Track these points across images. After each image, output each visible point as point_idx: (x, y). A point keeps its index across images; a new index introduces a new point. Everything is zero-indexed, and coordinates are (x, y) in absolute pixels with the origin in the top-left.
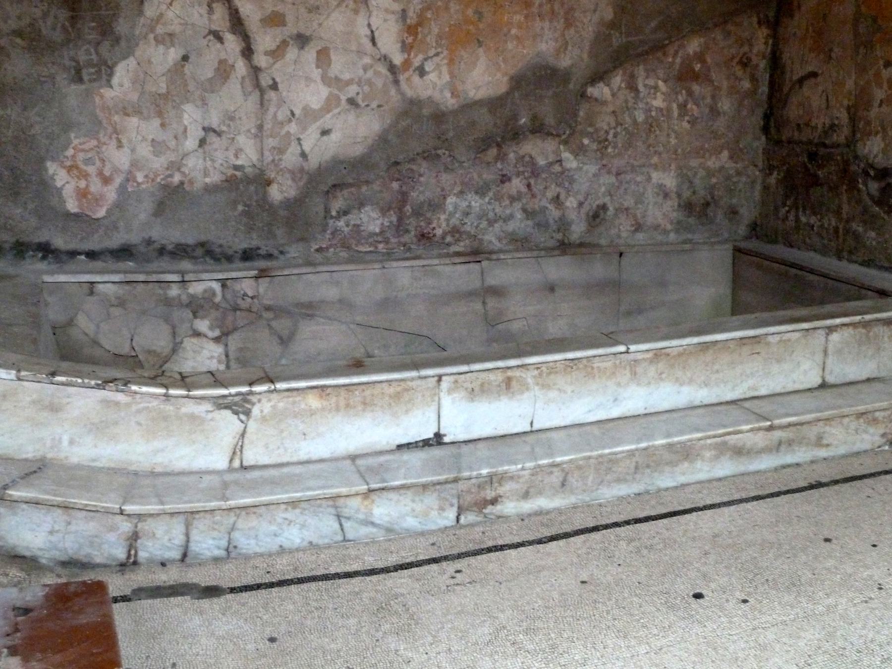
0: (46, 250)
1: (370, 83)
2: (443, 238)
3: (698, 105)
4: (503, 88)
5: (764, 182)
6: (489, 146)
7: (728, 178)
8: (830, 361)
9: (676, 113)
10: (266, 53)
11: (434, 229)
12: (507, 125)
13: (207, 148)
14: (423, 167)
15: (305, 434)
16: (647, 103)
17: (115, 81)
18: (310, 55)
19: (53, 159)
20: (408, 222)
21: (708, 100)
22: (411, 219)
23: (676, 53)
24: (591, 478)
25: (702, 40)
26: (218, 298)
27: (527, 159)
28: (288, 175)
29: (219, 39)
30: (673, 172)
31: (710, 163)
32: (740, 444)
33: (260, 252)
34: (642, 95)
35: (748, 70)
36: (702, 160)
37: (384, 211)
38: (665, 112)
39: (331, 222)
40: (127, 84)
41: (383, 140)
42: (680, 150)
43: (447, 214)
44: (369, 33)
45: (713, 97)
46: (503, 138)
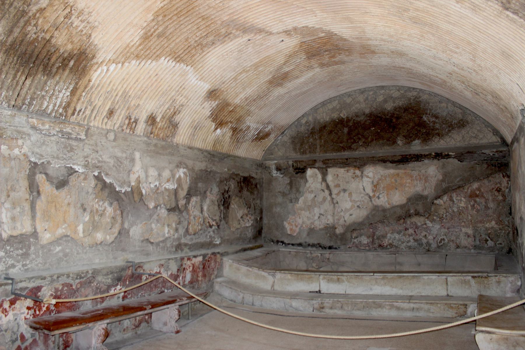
0: (283, 242)
1: (363, 201)
2: (387, 246)
3: (479, 206)
6: (401, 219)
7: (496, 231)
8: (449, 287)
9: (470, 208)
10: (335, 194)
12: (406, 212)
14: (380, 225)
16: (458, 205)
17: (299, 202)
18: (347, 194)
21: (484, 203)
23: (468, 188)
24: (350, 307)
25: (479, 184)
27: (414, 223)
28: (341, 226)
29: (323, 191)
31: (487, 225)
32: (398, 306)
34: (455, 203)
35: (501, 193)
36: (483, 224)
37: (368, 237)
39: (353, 240)
40: (302, 203)
41: (367, 217)
45: (486, 202)
46: (405, 217)
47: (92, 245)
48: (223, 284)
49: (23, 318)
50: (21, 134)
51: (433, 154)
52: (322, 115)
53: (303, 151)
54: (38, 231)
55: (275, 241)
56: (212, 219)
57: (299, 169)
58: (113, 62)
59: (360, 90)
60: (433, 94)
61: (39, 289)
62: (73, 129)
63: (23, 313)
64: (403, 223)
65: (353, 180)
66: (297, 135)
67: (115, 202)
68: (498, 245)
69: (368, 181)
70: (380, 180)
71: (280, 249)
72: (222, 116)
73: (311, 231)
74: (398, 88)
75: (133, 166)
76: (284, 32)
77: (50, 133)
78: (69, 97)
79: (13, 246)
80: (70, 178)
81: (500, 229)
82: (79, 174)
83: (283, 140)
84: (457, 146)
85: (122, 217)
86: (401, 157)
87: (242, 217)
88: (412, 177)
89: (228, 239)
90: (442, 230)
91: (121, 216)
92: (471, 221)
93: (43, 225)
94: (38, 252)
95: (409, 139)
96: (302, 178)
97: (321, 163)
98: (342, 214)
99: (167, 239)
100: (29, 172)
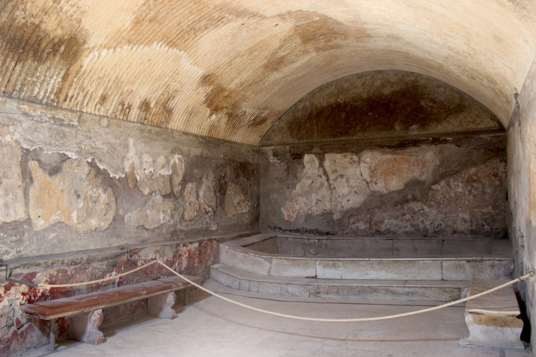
0: (280, 229)
1: (360, 187)
3: (476, 191)
4: (402, 187)
6: (398, 205)
7: (492, 216)
8: (444, 272)
10: (333, 180)
12: (404, 198)
13: (317, 205)
14: (377, 210)
16: (455, 190)
17: (296, 188)
18: (344, 180)
19: (283, 207)
21: (481, 189)
23: (465, 173)
25: (476, 169)
26: (317, 244)
29: (321, 177)
30: (467, 214)
31: (483, 211)
34: (452, 188)
35: (497, 178)
37: (366, 223)
38: (463, 193)
39: (350, 226)
40: (299, 189)
41: (365, 203)
42: (470, 206)
44: (360, 173)
45: (483, 188)
47: (87, 231)
48: (220, 270)
49: (19, 303)
50: (13, 121)
51: (431, 139)
52: (319, 100)
53: (300, 137)
54: (32, 217)
55: (272, 227)
56: (208, 205)
57: (296, 154)
58: (105, 48)
59: (357, 74)
60: (431, 79)
61: (33, 275)
62: (66, 116)
63: (19, 299)
64: (401, 208)
65: (350, 166)
66: (294, 121)
67: (110, 189)
68: (494, 230)
69: (365, 167)
70: (377, 165)
71: (278, 236)
72: (217, 102)
73: (309, 217)
74: (395, 72)
75: (127, 152)
76: (278, 16)
77: (42, 120)
78: (61, 83)
79: (7, 233)
80: (63, 165)
81: (497, 214)
82: (72, 161)
83: (280, 126)
84: (454, 131)
85: (117, 204)
86: (398, 142)
87: (238, 204)
88: (409, 162)
89: (224, 226)
90: (439, 216)
91: (115, 202)
92: (468, 207)
93: (36, 212)
94: (33, 239)
95: (407, 123)
96: (299, 164)
97: (318, 149)
98: (339, 199)
99: (162, 225)
100: (22, 159)
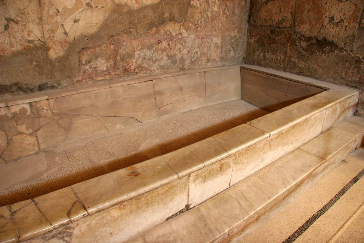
2: (134, 70)
5: (248, 41)
6: (153, 27)
9: (221, 14)
11: (130, 66)
12: (160, 17)
14: (125, 37)
15: (111, 233)
16: (212, 9)
20: (119, 64)
21: (232, 9)
22: (120, 63)
26: (29, 112)
33: (48, 85)
34: (210, 5)
36: (229, 33)
37: (108, 60)
39: (83, 67)
41: (105, 25)
42: (222, 29)
43: (136, 58)
45: (233, 7)
46: (158, 23)
81: (240, 38)
